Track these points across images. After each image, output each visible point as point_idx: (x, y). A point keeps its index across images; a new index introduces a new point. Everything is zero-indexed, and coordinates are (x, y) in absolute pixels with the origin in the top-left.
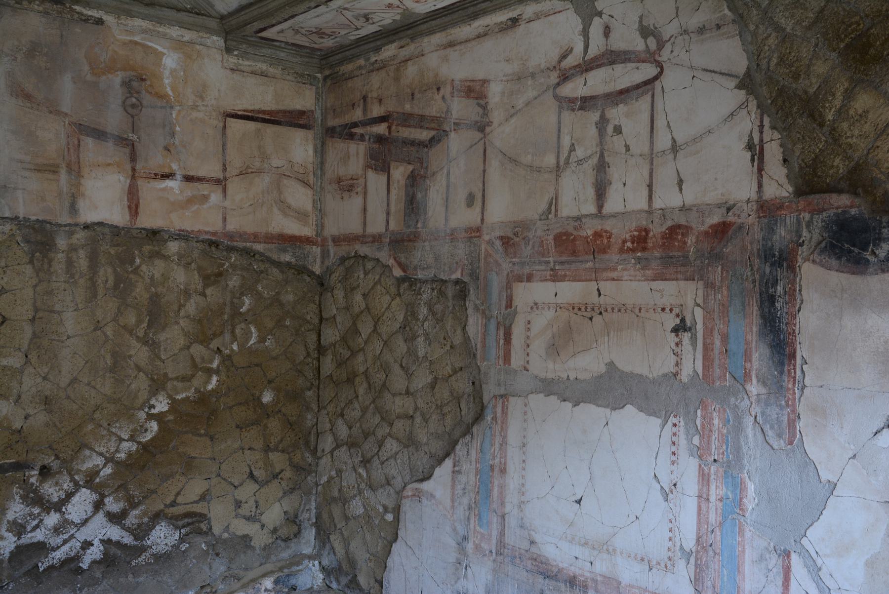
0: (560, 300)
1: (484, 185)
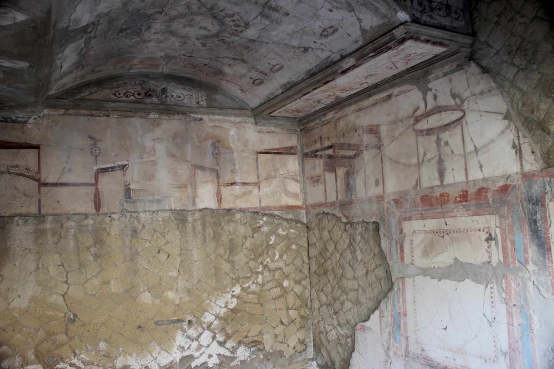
0: (426, 228)
1: (383, 175)
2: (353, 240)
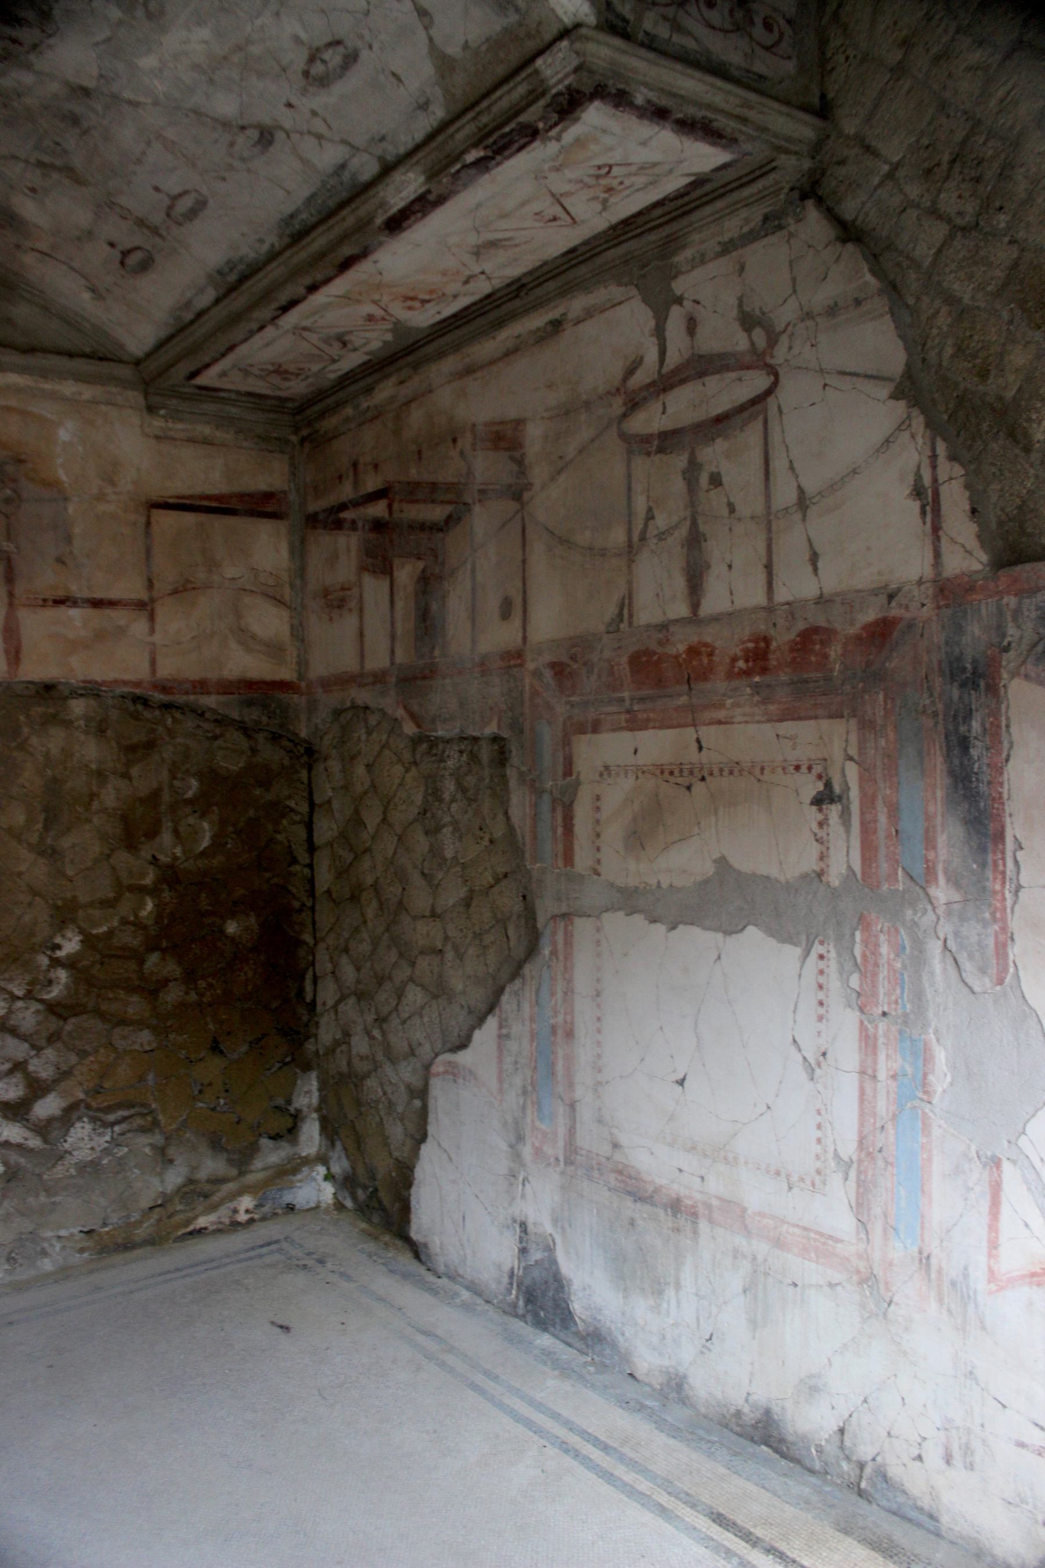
0: (642, 759)
1: (524, 584)
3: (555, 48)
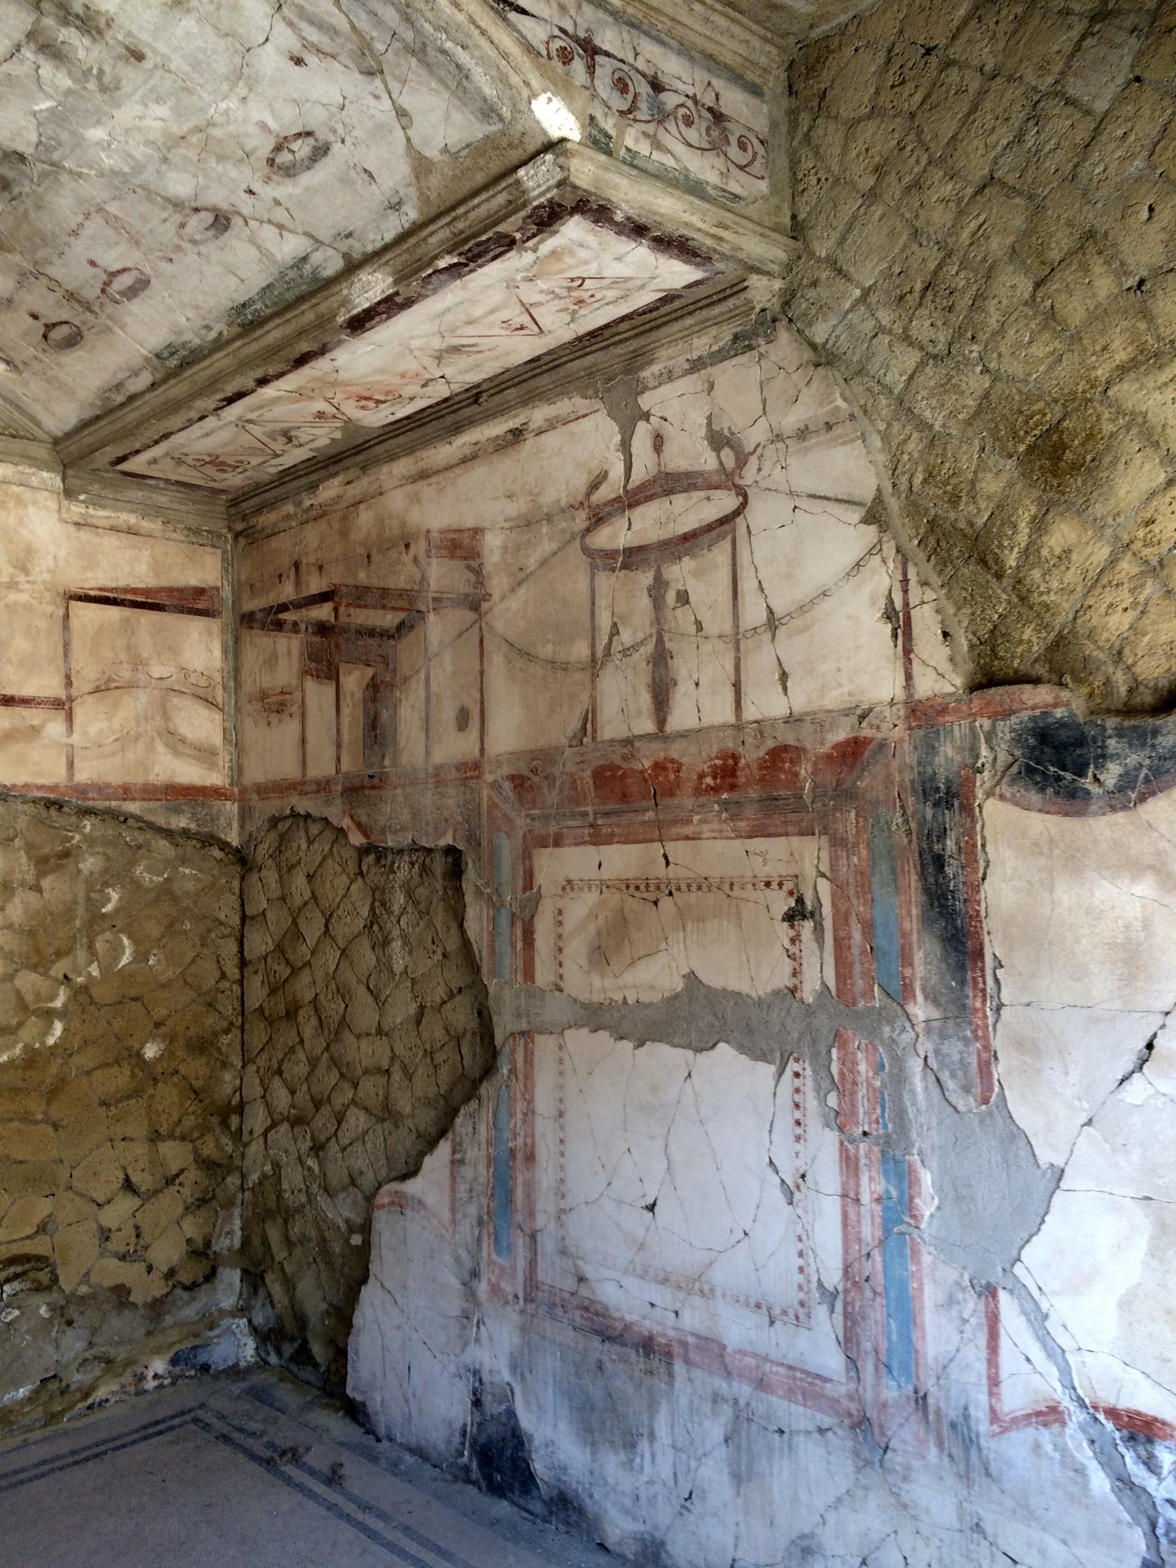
0: (605, 874)
2: (383, 904)
3: (539, 160)
